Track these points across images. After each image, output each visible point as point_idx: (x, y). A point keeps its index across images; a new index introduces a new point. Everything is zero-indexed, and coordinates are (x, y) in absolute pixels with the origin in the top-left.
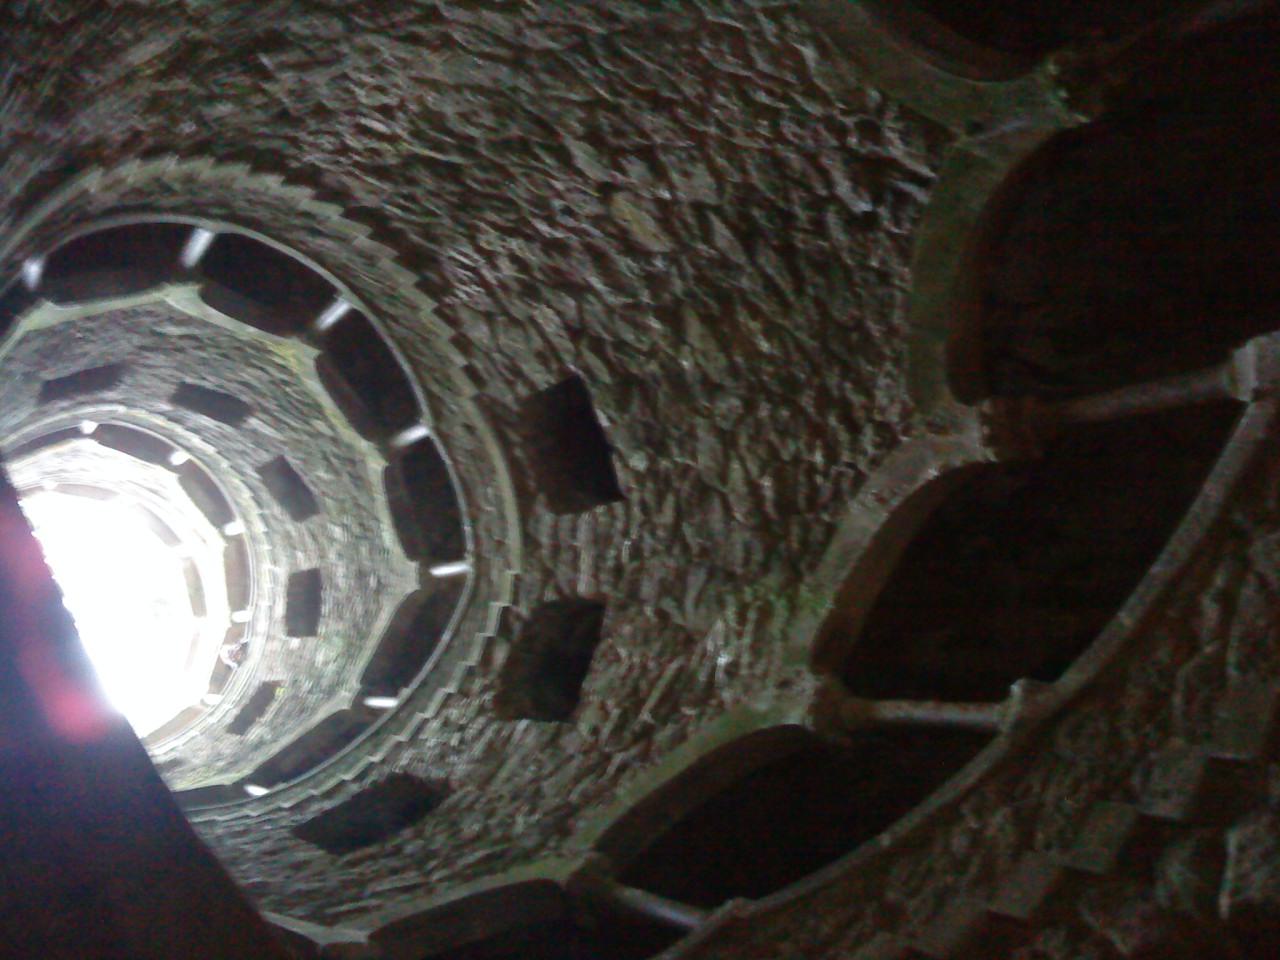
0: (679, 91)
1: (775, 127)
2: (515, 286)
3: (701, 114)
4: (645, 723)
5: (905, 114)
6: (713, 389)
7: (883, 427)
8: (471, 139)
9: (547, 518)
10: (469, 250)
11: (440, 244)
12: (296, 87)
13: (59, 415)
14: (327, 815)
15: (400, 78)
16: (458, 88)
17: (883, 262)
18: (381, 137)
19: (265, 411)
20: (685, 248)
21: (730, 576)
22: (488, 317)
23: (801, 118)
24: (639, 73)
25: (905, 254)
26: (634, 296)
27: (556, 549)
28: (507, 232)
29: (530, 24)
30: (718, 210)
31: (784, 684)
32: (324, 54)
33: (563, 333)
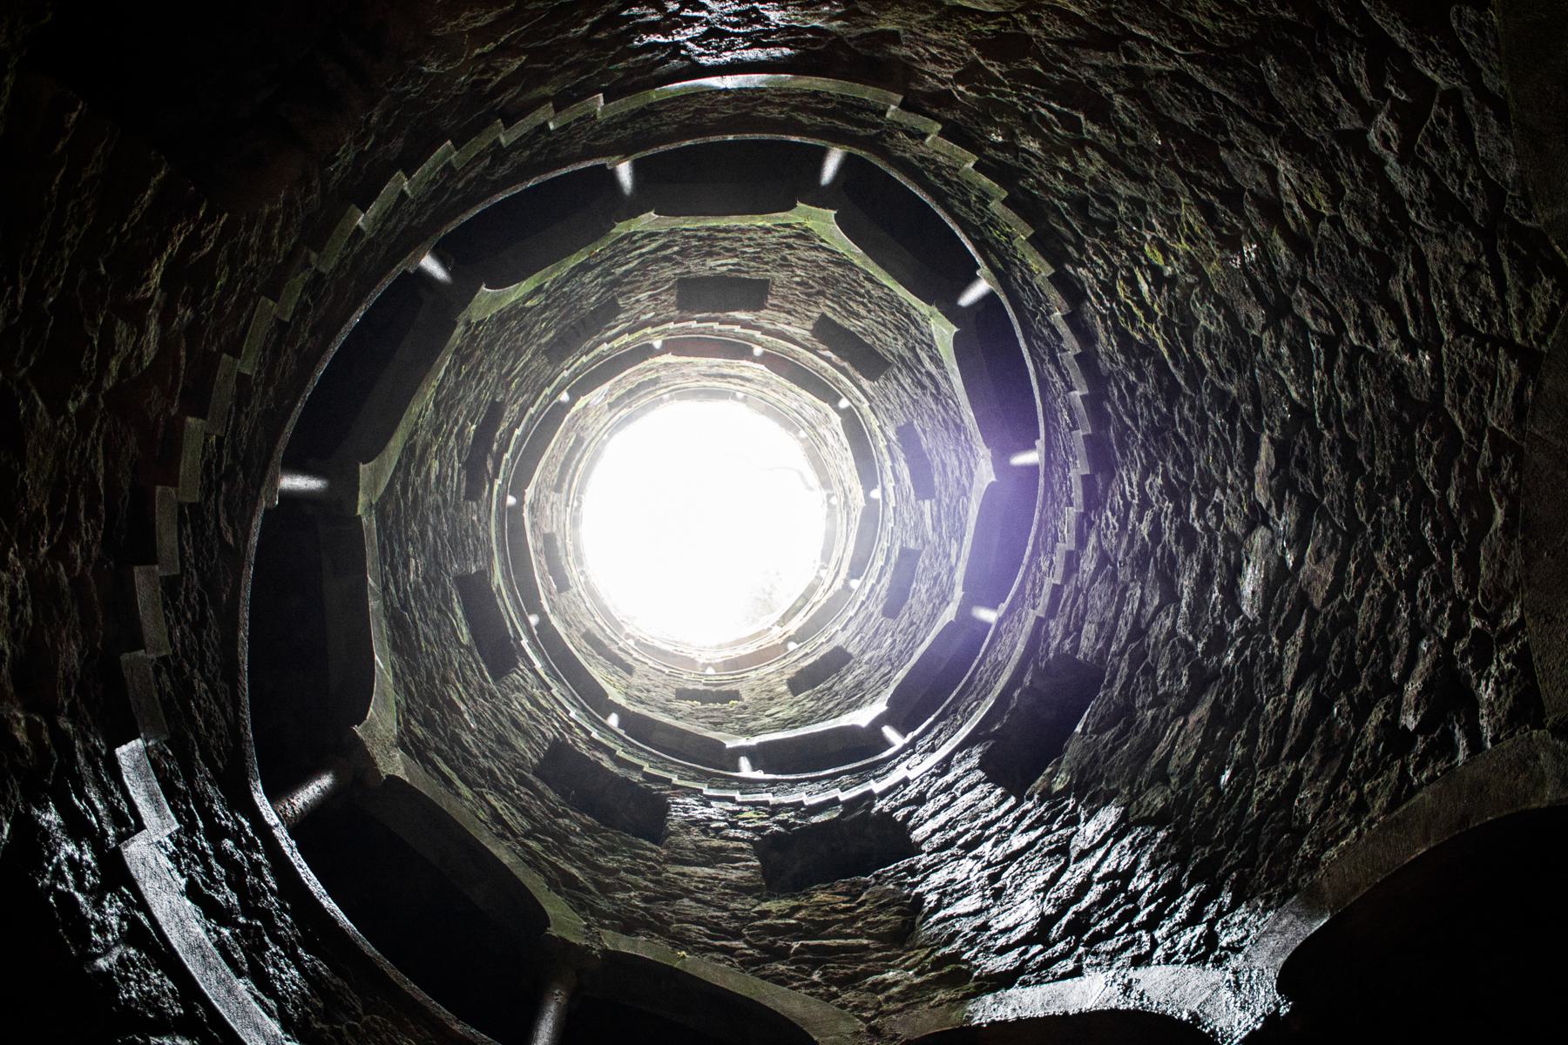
0: (1371, 462)
2: (1137, 547)
3: (1372, 506)
4: (790, 947)
5: (1522, 659)
7: (1211, 939)
8: (1203, 371)
9: (975, 761)
10: (1135, 479)
11: (1123, 455)
12: (1100, 178)
13: (822, 362)
14: (597, 765)
15: (1182, 247)
16: (1220, 302)
17: (1373, 792)
18: (1141, 303)
19: (939, 502)
20: (1264, 629)
21: (985, 927)
22: (1104, 559)
23: (1442, 584)
24: (1355, 415)
25: (1394, 804)
26: (1197, 639)
27: (949, 787)
28: (1170, 490)
29: (1305, 283)
30: (1314, 614)
32: (1131, 160)
33: (1130, 619)
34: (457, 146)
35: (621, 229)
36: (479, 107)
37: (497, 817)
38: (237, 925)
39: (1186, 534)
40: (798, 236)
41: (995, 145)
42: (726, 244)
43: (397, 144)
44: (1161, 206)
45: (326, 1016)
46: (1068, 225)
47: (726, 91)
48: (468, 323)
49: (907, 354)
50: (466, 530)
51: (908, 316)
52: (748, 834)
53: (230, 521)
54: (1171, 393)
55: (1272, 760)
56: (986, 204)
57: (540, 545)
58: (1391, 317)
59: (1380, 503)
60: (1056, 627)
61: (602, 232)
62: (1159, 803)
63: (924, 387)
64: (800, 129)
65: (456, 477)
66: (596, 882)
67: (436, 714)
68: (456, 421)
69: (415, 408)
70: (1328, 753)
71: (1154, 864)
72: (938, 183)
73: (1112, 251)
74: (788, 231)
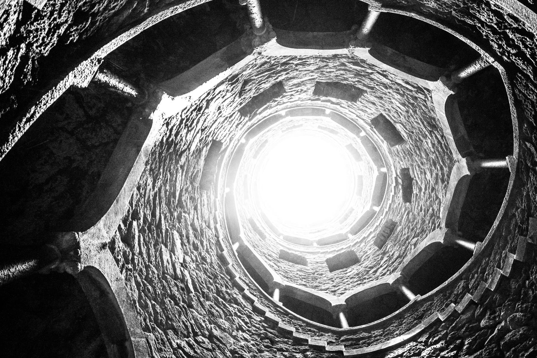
1: (148, 273)
2: (204, 236)
3: (164, 287)
6: (182, 167)
7: (168, 124)
9: (224, 144)
10: (213, 258)
11: (218, 263)
15: (243, 343)
16: (224, 330)
18: (240, 317)
22: (209, 227)
28: (204, 259)
30: (163, 243)
31: (260, 53)
34: (488, 290)
35: (397, 274)
36: (487, 303)
37: (385, 76)
38: (509, 29)
39: (196, 248)
40: (335, 291)
41: (306, 350)
42: (355, 280)
43: (514, 285)
44: (255, 354)
45: (468, 8)
46: (271, 333)
47: (398, 335)
48: (441, 228)
49: (279, 264)
50: (404, 158)
51: (287, 278)
52: (287, 94)
53: (529, 149)
54: (219, 292)
55: (160, 189)
56: (297, 329)
57: (363, 158)
58: (188, 353)
59: (162, 289)
60: (212, 197)
61: (404, 270)
62: (182, 159)
63: (269, 255)
64: (364, 330)
65: (415, 174)
66: (346, 66)
67: (412, 101)
68: (424, 193)
69: (450, 196)
70: (149, 201)
71: (182, 140)
72: (312, 329)
73: (256, 331)
74: (339, 292)
